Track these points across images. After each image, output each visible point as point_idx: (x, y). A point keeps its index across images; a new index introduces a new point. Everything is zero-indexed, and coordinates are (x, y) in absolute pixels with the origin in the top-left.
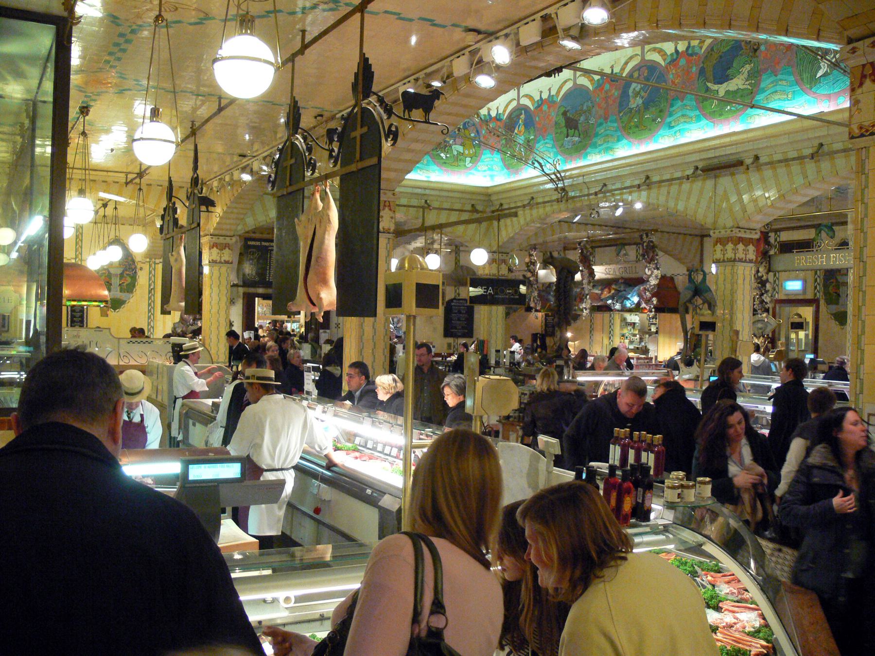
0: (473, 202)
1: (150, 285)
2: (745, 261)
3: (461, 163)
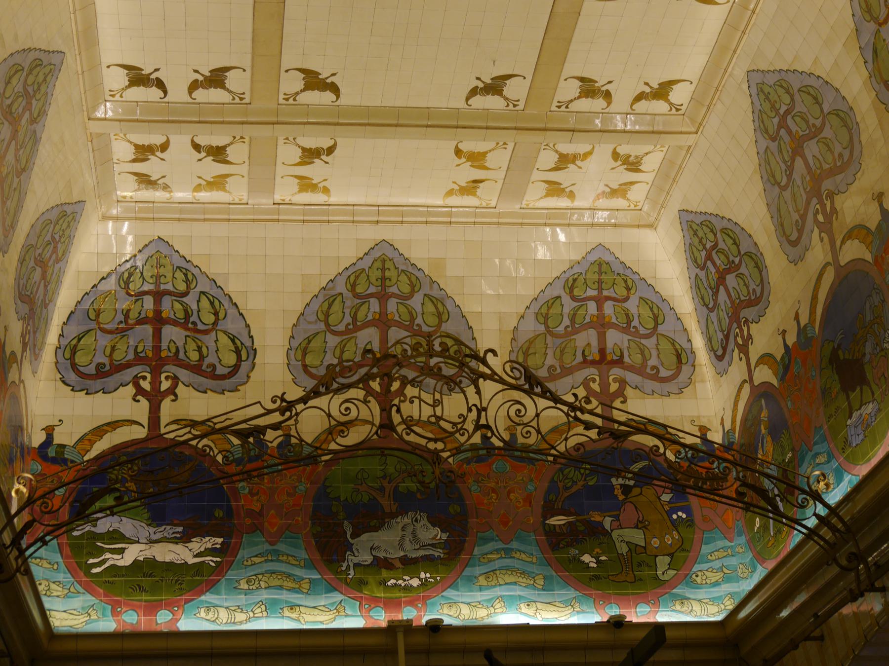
3: (646, 572)
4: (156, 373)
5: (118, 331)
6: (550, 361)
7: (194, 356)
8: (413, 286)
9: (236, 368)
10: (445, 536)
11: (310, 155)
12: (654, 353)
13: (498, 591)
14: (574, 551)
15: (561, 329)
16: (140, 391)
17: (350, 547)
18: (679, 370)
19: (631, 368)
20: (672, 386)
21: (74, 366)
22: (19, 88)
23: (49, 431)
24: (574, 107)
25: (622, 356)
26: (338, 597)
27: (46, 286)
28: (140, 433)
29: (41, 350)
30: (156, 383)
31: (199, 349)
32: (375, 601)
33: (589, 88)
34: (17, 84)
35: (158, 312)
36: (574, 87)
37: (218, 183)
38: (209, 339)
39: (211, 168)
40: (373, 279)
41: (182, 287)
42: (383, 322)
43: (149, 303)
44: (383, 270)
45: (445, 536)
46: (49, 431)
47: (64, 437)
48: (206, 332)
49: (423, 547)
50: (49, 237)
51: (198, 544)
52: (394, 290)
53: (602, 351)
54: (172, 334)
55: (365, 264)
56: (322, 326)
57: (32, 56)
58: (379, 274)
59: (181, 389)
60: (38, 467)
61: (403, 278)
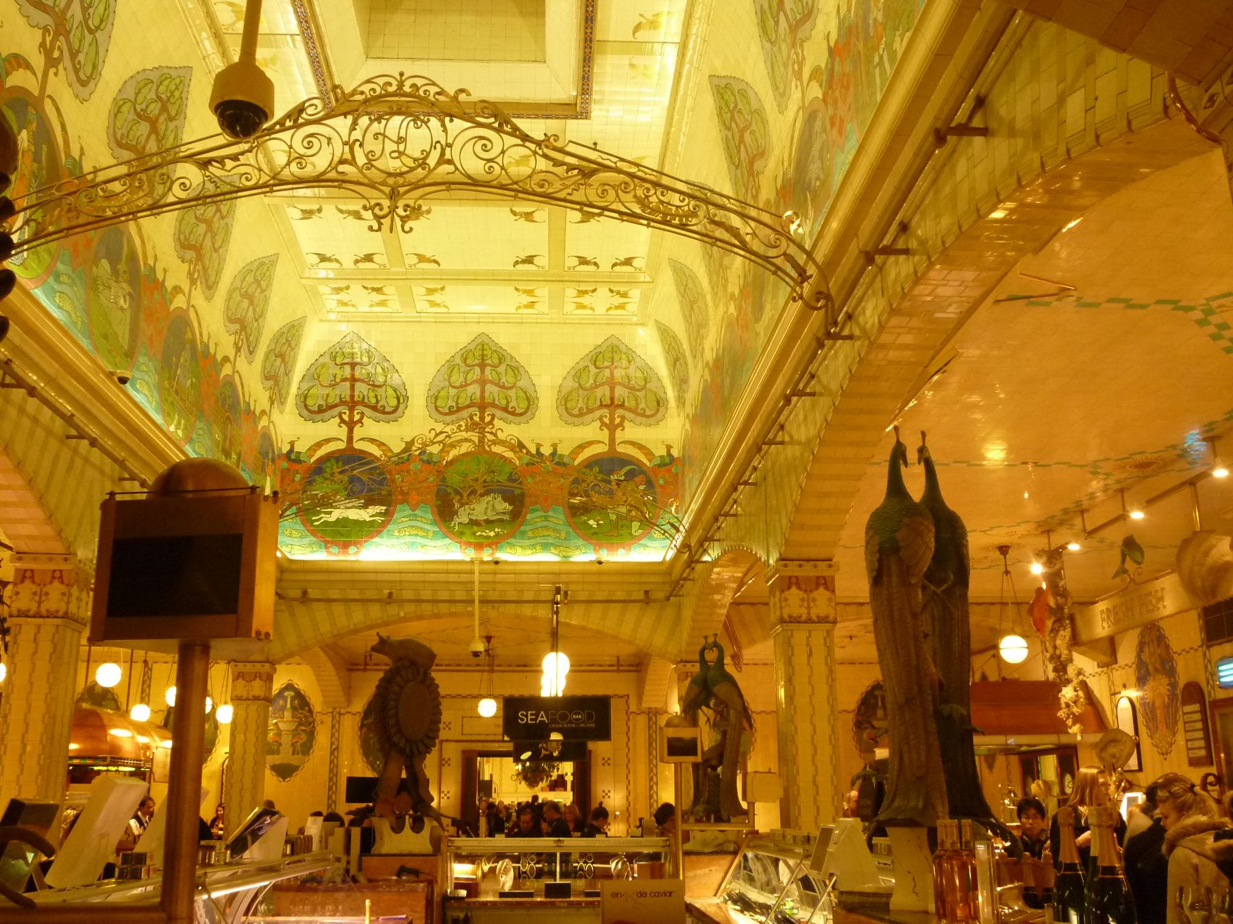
0: (647, 587)
1: (332, 743)
2: (809, 621)
3: (624, 532)
4: (351, 410)
5: (331, 386)
6: (580, 405)
7: (373, 401)
8: (500, 360)
9: (397, 408)
10: (511, 508)
11: (431, 291)
12: (644, 400)
13: (539, 540)
14: (585, 518)
15: (588, 385)
16: (342, 421)
17: (456, 513)
18: (658, 410)
19: (630, 410)
20: (653, 420)
21: (306, 406)
22: (252, 280)
23: (292, 444)
24: (576, 269)
25: (624, 402)
26: (448, 541)
27: (285, 366)
28: (342, 445)
29: (285, 398)
30: (351, 416)
31: (376, 396)
32: (469, 544)
33: (583, 261)
34: (250, 279)
35: (353, 375)
37: (382, 303)
38: (381, 392)
39: (376, 297)
40: (477, 355)
41: (365, 359)
43: (348, 369)
44: (483, 350)
45: (511, 508)
46: (292, 444)
47: (301, 447)
48: (380, 386)
49: (498, 514)
50: (284, 341)
52: (489, 362)
53: (612, 399)
54: (361, 388)
55: (472, 347)
56: (447, 383)
57: (257, 263)
58: (481, 353)
59: (365, 420)
60: (285, 465)
61: (495, 355)
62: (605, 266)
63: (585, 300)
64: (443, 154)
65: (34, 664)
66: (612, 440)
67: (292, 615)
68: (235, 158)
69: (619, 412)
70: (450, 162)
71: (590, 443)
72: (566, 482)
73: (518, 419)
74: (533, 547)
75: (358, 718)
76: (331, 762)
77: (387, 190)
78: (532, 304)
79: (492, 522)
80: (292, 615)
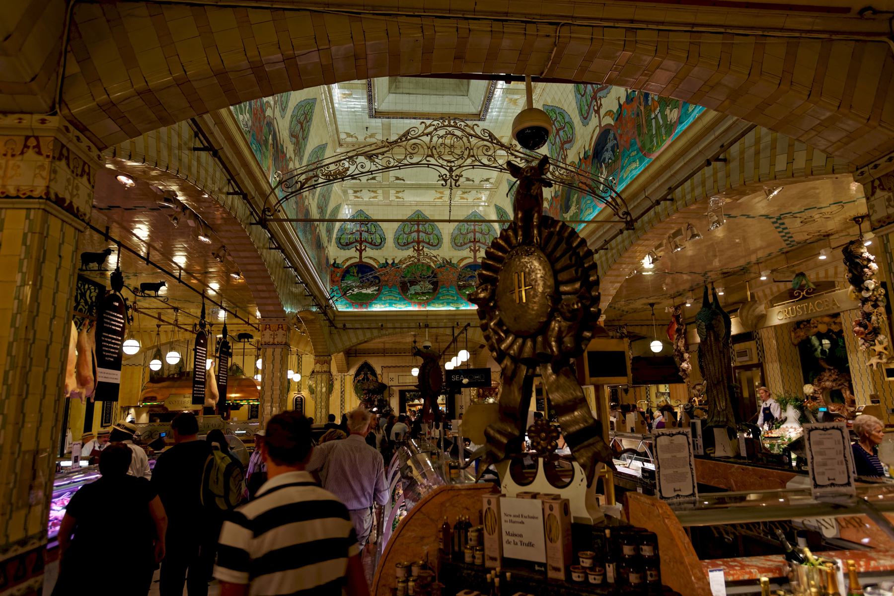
4: (361, 244)
6: (461, 241)
7: (370, 240)
9: (381, 243)
16: (357, 249)
19: (482, 243)
23: (335, 260)
28: (357, 260)
30: (361, 247)
32: (415, 303)
33: (468, 179)
36: (465, 179)
39: (373, 194)
42: (418, 231)
46: (335, 260)
47: (339, 261)
51: (372, 289)
53: (475, 239)
59: (367, 249)
60: (333, 269)
62: (477, 182)
63: (465, 196)
64: (469, 153)
65: (273, 365)
66: (475, 257)
67: (340, 335)
68: (383, 154)
69: (478, 244)
70: (473, 156)
71: (466, 258)
72: (456, 275)
73: (434, 248)
74: (443, 303)
75: (353, 377)
76: (341, 397)
77: (448, 168)
78: (441, 198)
79: (425, 293)
80: (340, 335)
